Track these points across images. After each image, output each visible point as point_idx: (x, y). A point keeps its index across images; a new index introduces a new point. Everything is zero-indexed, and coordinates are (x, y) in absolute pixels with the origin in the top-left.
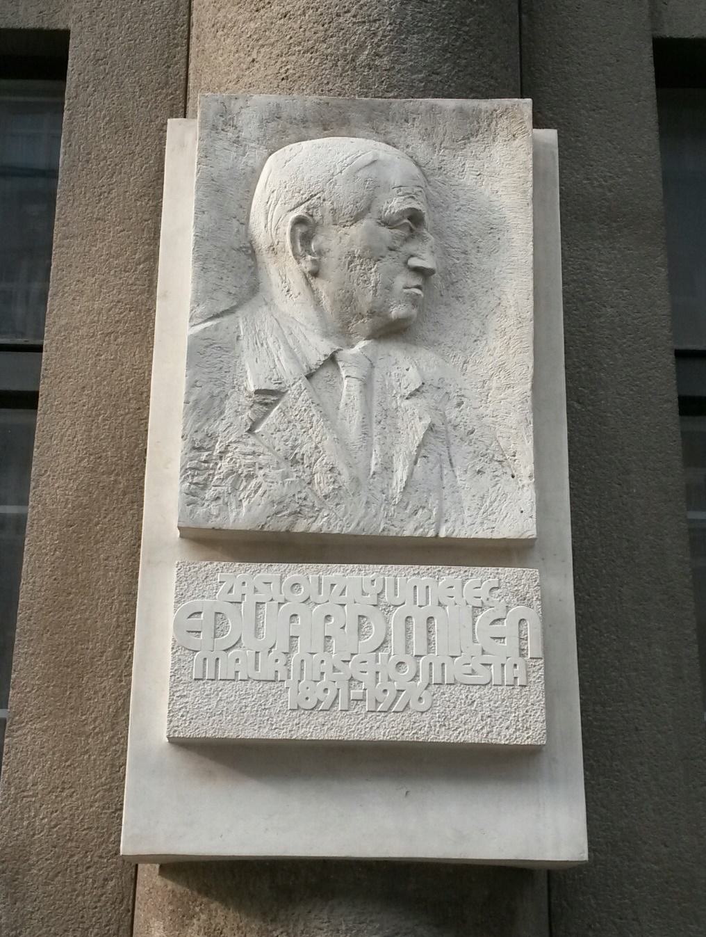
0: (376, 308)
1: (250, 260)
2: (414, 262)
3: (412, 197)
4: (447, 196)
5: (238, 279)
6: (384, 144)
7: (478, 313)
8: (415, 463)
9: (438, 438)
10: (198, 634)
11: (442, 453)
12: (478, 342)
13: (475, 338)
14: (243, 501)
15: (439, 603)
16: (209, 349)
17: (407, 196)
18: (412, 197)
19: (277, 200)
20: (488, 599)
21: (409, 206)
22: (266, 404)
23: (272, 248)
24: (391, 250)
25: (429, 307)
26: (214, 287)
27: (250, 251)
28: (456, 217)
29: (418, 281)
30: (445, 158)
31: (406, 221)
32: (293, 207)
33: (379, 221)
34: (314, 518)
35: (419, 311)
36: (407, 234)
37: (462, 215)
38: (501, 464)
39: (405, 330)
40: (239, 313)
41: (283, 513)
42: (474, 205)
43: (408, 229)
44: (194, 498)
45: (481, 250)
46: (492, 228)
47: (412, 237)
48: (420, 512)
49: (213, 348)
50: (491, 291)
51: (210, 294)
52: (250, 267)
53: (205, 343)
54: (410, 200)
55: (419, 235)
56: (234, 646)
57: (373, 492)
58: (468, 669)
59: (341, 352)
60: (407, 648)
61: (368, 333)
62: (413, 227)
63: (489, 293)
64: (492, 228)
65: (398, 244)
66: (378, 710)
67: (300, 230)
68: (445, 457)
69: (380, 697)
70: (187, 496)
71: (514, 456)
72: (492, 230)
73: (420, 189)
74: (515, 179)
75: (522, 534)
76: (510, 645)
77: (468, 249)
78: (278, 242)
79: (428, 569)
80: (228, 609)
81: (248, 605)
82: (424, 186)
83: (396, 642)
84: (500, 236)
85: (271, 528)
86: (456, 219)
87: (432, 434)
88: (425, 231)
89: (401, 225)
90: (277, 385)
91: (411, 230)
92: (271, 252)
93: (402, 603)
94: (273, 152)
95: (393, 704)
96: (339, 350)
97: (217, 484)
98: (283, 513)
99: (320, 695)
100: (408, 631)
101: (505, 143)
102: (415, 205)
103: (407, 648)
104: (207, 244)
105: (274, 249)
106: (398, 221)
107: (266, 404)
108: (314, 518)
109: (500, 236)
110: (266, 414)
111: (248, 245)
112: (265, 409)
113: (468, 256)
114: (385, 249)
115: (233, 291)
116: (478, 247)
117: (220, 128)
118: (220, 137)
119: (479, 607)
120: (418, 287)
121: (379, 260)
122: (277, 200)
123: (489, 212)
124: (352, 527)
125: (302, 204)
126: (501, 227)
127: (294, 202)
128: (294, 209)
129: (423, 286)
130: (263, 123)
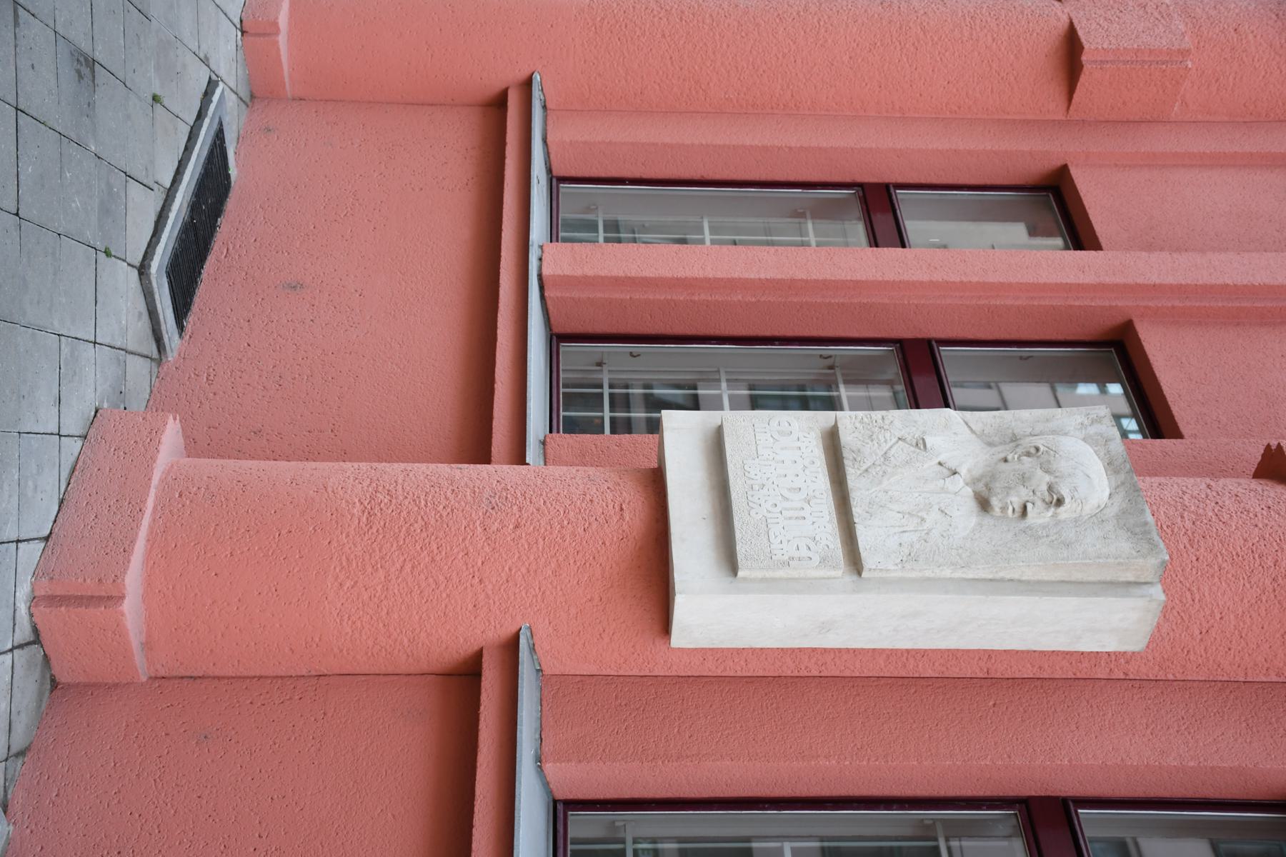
2: (1029, 506)
8: (899, 512)
22: (917, 445)
24: (1033, 491)
31: (1055, 497)
39: (985, 511)
40: (974, 436)
43: (1051, 499)
47: (1047, 504)
55: (1050, 507)
58: (777, 533)
60: (786, 509)
65: (1038, 494)
67: (1033, 451)
76: (796, 554)
81: (799, 444)
83: (787, 504)
87: (920, 520)
96: (961, 476)
102: (1067, 500)
103: (786, 509)
110: (911, 445)
112: (915, 445)
127: (1049, 445)
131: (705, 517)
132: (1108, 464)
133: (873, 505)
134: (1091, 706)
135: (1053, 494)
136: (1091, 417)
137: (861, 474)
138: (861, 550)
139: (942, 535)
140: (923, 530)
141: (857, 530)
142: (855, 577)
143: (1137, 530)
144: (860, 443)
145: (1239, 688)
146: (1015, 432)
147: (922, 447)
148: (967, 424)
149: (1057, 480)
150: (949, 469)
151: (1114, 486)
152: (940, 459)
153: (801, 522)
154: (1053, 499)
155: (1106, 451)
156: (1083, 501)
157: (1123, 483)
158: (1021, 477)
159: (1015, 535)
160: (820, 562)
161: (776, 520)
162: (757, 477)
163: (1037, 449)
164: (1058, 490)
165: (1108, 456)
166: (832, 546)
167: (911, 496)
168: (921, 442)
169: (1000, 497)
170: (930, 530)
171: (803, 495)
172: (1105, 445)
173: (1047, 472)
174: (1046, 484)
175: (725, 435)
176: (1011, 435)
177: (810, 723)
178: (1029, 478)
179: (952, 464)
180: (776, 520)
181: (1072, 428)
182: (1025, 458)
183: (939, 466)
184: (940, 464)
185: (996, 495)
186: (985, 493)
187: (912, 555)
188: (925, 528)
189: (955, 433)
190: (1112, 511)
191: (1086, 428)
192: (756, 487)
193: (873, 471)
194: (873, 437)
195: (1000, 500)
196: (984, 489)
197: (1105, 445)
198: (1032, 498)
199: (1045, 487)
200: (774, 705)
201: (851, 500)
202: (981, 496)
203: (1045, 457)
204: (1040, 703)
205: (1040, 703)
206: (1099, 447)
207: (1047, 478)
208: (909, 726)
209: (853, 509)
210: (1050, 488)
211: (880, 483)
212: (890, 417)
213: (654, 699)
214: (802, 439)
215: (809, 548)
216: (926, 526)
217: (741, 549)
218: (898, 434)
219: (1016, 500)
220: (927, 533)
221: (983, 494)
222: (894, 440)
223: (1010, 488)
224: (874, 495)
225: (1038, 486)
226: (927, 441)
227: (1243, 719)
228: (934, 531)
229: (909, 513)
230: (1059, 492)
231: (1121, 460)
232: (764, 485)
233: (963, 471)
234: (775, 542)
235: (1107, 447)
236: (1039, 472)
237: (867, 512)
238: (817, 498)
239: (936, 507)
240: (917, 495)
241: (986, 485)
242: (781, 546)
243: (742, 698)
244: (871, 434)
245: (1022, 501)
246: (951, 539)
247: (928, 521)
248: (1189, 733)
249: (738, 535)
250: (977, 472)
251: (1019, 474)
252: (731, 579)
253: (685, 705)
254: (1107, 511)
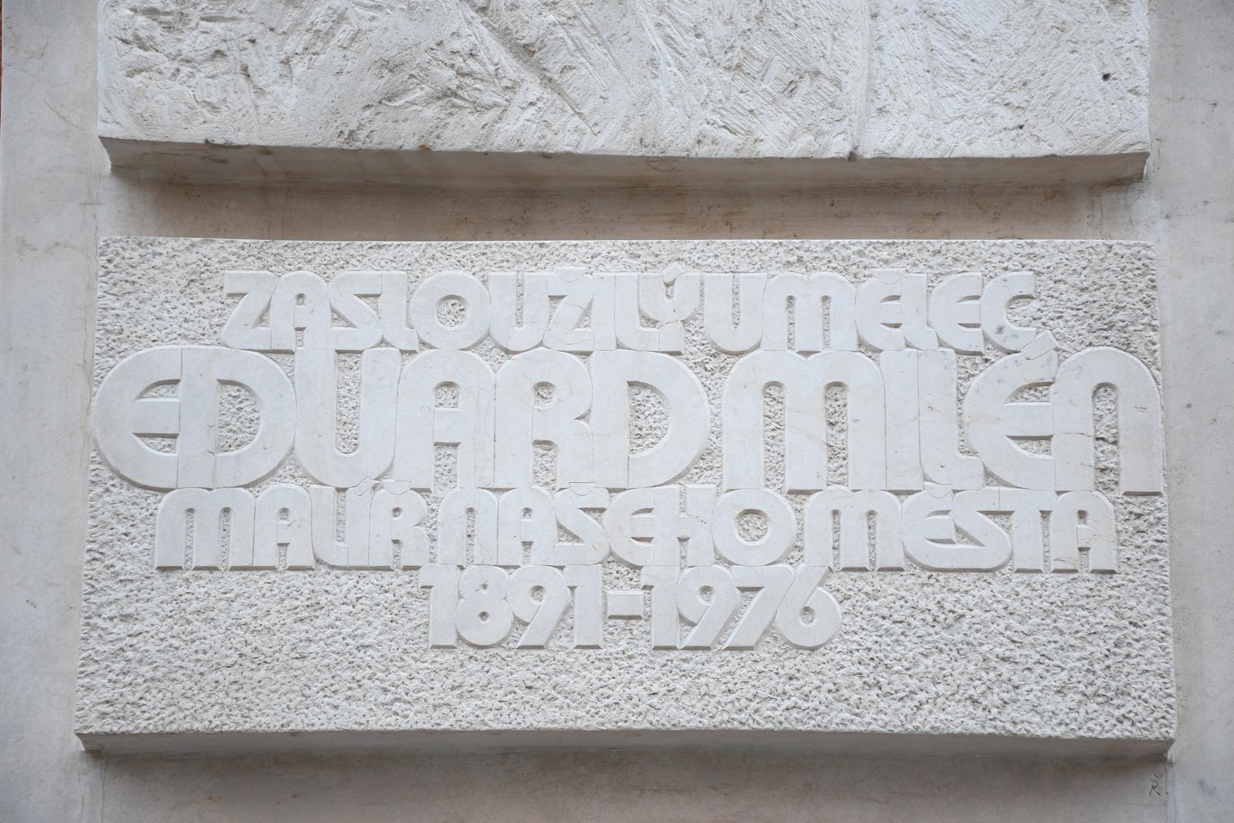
10: (168, 441)
14: (295, 60)
15: (861, 343)
20: (1000, 330)
34: (497, 111)
41: (411, 97)
44: (146, 54)
48: (804, 87)
56: (273, 473)
57: (668, 30)
58: (943, 526)
60: (775, 468)
66: (686, 643)
69: (695, 605)
70: (126, 48)
75: (1107, 141)
79: (828, 249)
80: (255, 371)
85: (376, 139)
93: (752, 344)
95: (726, 629)
97: (213, 13)
98: (411, 97)
99: (524, 605)
100: (774, 426)
108: (497, 111)
119: (975, 354)
124: (606, 134)
133: (749, 55)
137: (548, 82)
138: (1027, 149)
141: (900, 153)
142: (1147, 204)
144: (330, 55)
153: (855, 405)
160: (1127, 346)
161: (852, 523)
162: (556, 585)
166: (1022, 282)
175: (233, 723)
180: (852, 523)
192: (625, 598)
201: (704, 151)
209: (769, 148)
214: (280, 332)
215: (1034, 386)
224: (688, 43)
232: (612, 558)
238: (697, 314)
242: (1026, 519)
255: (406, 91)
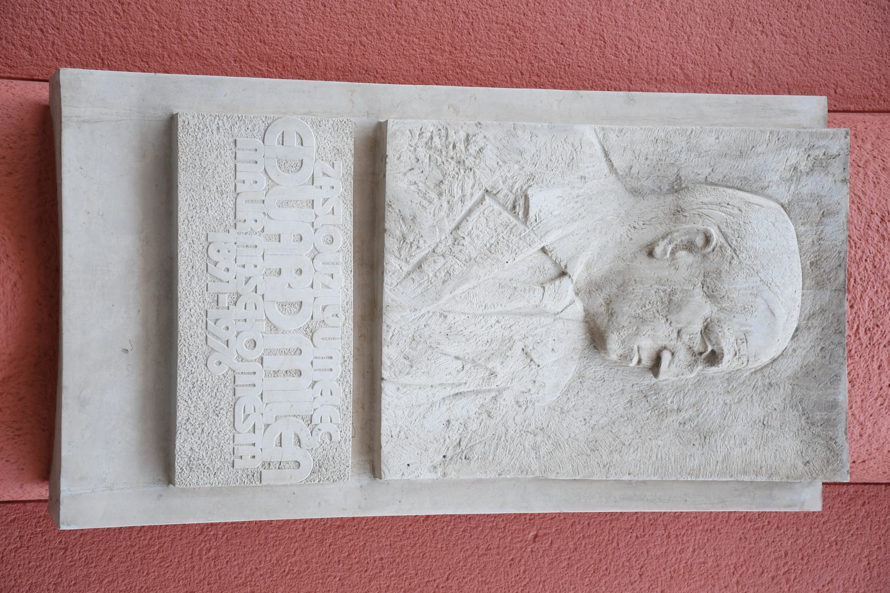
0: (617, 317)
1: (667, 187)
2: (666, 357)
3: (736, 354)
4: (740, 391)
5: (646, 175)
6: (795, 326)
7: (614, 423)
8: (457, 358)
9: (483, 381)
10: (281, 142)
11: (467, 386)
12: (583, 423)
13: (588, 419)
14: (416, 186)
15: (315, 382)
16: (570, 147)
17: (737, 349)
18: (736, 354)
19: (731, 215)
20: (319, 430)
21: (726, 351)
22: (514, 207)
23: (679, 209)
24: (679, 332)
25: (620, 372)
26: (637, 152)
27: (676, 187)
28: (718, 400)
29: (647, 362)
30: (782, 390)
31: (710, 349)
32: (723, 231)
33: (709, 320)
34: (398, 256)
35: (616, 362)
36: (696, 349)
37: (719, 406)
38: (457, 445)
41: (403, 226)
42: (730, 419)
43: (702, 349)
44: (417, 136)
45: (682, 426)
46: (705, 437)
47: (694, 354)
48: (407, 362)
49: (572, 152)
50: (637, 437)
51: (629, 146)
52: (660, 187)
53: (577, 144)
54: (733, 353)
56: (270, 178)
57: (427, 315)
59: (570, 281)
60: (271, 352)
61: (591, 311)
62: (704, 355)
63: (635, 434)
64: (705, 437)
65: (685, 338)
66: (208, 321)
68: (462, 389)
69: (222, 325)
70: (419, 129)
71: (465, 458)
72: (703, 437)
73: (745, 363)
74: (759, 462)
75: (386, 465)
76: (275, 454)
77: (683, 413)
78: (686, 216)
79: (349, 371)
80: (306, 172)
81: (312, 193)
82: (750, 366)
83: (276, 341)
84: (697, 445)
85: (388, 214)
86: (716, 400)
87: (488, 373)
88: (700, 367)
89: (705, 343)
90: (534, 218)
91: (701, 354)
92: (676, 208)
93: (315, 345)
94: (785, 209)
95: (214, 335)
96: (572, 280)
97: (432, 159)
99: (222, 265)
100: (286, 352)
101: (799, 453)
102: (726, 358)
103: (271, 352)
104: (683, 143)
105: (679, 212)
106: (709, 339)
107: (514, 207)
108: (398, 256)
109: (697, 445)
111: (684, 185)
112: (510, 206)
113: (676, 413)
114: (679, 326)
115: (634, 170)
116: (685, 423)
117: (810, 153)
118: (801, 153)
119: (311, 421)
120: (639, 362)
121: (667, 320)
122: (731, 215)
123: (723, 435)
124: (391, 294)
125: (726, 240)
126: (706, 447)
127: (729, 232)
128: (721, 231)
129: (641, 366)
130: (817, 198)
131: (129, 348)
132: (812, 264)
133: (418, 343)
134: (669, 537)
135: (708, 343)
136: (815, 153)
137: (409, 274)
138: (384, 439)
139: (517, 402)
140: (489, 391)
141: (383, 396)
142: (366, 479)
143: (818, 416)
144: (418, 198)
145: (876, 496)
146: (683, 173)
147: (521, 215)
148: (606, 155)
149: (722, 316)
150: (555, 263)
151: (807, 311)
152: (546, 242)
153: (293, 380)
154: (705, 351)
155: (816, 237)
156: (750, 359)
157: (823, 311)
158: (666, 300)
159: (630, 401)
160: (313, 472)
161: (251, 379)
162: (229, 276)
163: (708, 240)
164: (717, 338)
165: (816, 248)
166: (337, 437)
167: (483, 323)
168: (521, 202)
169: (624, 333)
170: (500, 392)
171: (302, 319)
172: (819, 223)
173: (711, 296)
174: (702, 321)
175: (181, 165)
176: (673, 179)
177: (262, 582)
178: (679, 307)
179: (562, 253)
180: (251, 379)
181: (776, 178)
182: (682, 254)
183: (541, 254)
184: (543, 250)
185: (618, 330)
186: (602, 321)
187: (463, 444)
188: (494, 387)
189: (583, 178)
190: (788, 367)
191: (799, 180)
192: (225, 300)
193: (429, 269)
194: (443, 187)
195: (623, 342)
196: (603, 309)
197: (819, 223)
198: (673, 343)
199: (698, 327)
200: (212, 551)
201: (384, 328)
202: (594, 321)
203: (715, 258)
204: (599, 532)
205: (599, 532)
206: (808, 226)
207: (707, 310)
208: (407, 582)
209: (385, 350)
210: (707, 331)
211: (438, 296)
212: (479, 138)
213: (17, 549)
214: (320, 180)
215: (299, 441)
216: (499, 382)
217: (183, 444)
218: (487, 184)
219: (646, 346)
220: (495, 398)
221: (598, 322)
222: (478, 194)
223: (643, 320)
224: (422, 322)
225: (689, 323)
226: (532, 202)
227: (866, 552)
228: (506, 394)
229: (473, 361)
230: (718, 343)
231: (833, 263)
232: (239, 296)
233: (578, 271)
234: (243, 427)
235: (821, 228)
236: (698, 296)
237: (406, 358)
238: (326, 325)
239: (519, 346)
240: (493, 320)
241: (609, 303)
242: (252, 438)
243: (163, 540)
244: (441, 178)
245: (656, 347)
246: (530, 411)
247: (499, 377)
248: (788, 581)
249: (182, 414)
250: (597, 272)
251: (665, 291)
252: (159, 489)
253: (69, 559)
254: (782, 364)
255: (405, 224)
